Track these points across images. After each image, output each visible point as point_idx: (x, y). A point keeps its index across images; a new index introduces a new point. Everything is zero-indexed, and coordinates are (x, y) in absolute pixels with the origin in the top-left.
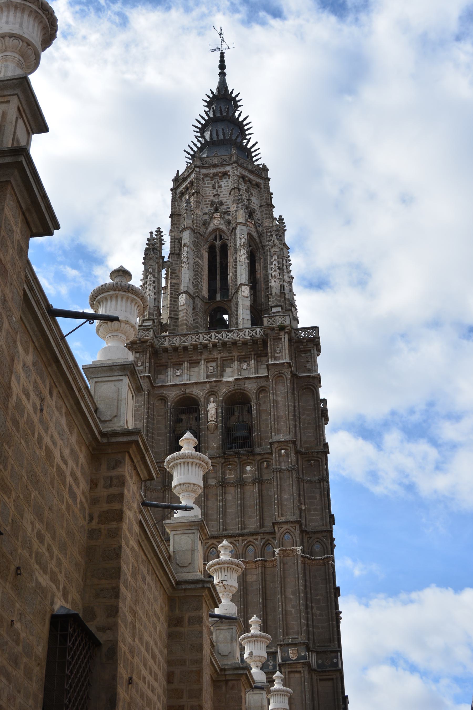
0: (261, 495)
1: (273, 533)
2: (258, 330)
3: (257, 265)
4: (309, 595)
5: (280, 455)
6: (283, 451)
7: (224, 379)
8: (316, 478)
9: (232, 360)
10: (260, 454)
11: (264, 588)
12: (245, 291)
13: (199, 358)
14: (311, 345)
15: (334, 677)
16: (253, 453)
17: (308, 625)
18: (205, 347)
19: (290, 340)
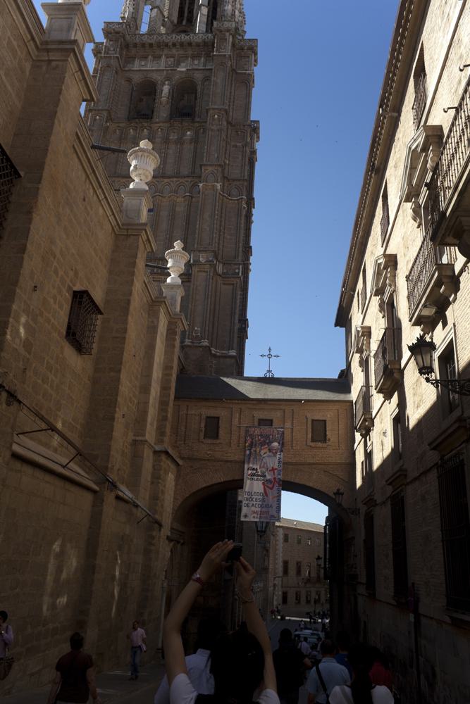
0: (195, 151)
1: (200, 177)
2: (210, 35)
3: (218, 10)
4: (223, 223)
5: (214, 119)
6: (216, 116)
7: (178, 69)
8: (240, 144)
9: (187, 57)
10: (198, 122)
11: (188, 216)
12: (205, 10)
13: (161, 53)
14: (250, 52)
15: (235, 282)
16: (193, 121)
17: (219, 244)
18: (167, 45)
19: (233, 45)
